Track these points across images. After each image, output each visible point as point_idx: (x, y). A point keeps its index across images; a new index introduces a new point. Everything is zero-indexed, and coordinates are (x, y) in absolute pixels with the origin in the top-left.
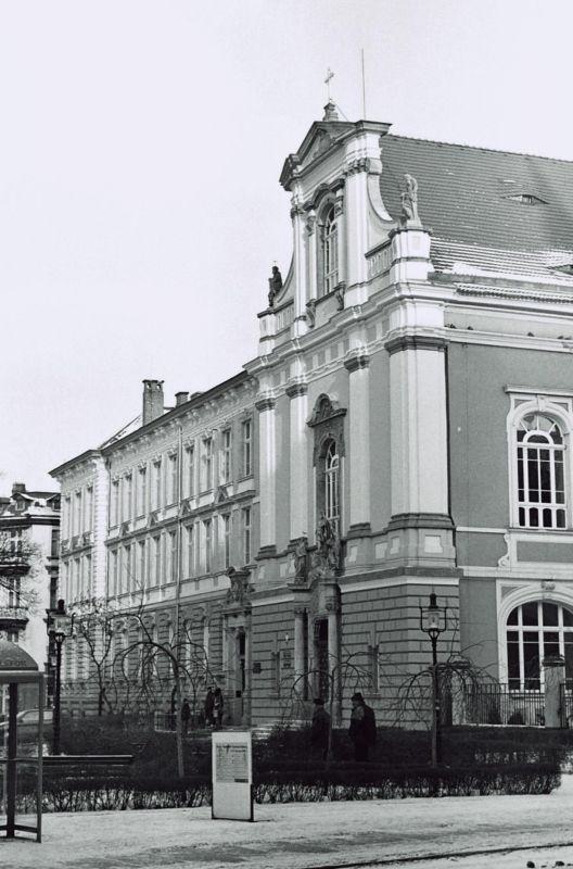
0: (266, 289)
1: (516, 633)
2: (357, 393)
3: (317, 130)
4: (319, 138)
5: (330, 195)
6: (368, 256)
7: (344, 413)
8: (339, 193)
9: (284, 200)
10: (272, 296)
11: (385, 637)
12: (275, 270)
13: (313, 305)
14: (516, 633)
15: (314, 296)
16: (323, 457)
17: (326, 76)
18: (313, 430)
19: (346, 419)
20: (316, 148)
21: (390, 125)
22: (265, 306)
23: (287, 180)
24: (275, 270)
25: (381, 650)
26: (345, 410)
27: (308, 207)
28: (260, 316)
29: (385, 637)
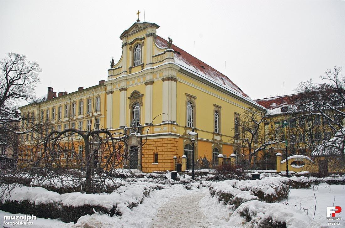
0: (110, 64)
1: (187, 151)
2: (147, 91)
3: (135, 25)
4: (135, 27)
5: (139, 41)
6: (153, 57)
7: (143, 95)
8: (143, 41)
9: (121, 42)
10: (112, 66)
11: (159, 150)
12: (113, 59)
13: (130, 69)
14: (187, 151)
15: (130, 66)
16: (132, 107)
17: (137, 12)
18: (129, 100)
19: (143, 97)
20: (134, 29)
21: (158, 27)
22: (110, 68)
23: (122, 37)
24: (113, 59)
25: (158, 153)
26: (143, 95)
27: (131, 43)
28: (108, 70)
29: (159, 150)
